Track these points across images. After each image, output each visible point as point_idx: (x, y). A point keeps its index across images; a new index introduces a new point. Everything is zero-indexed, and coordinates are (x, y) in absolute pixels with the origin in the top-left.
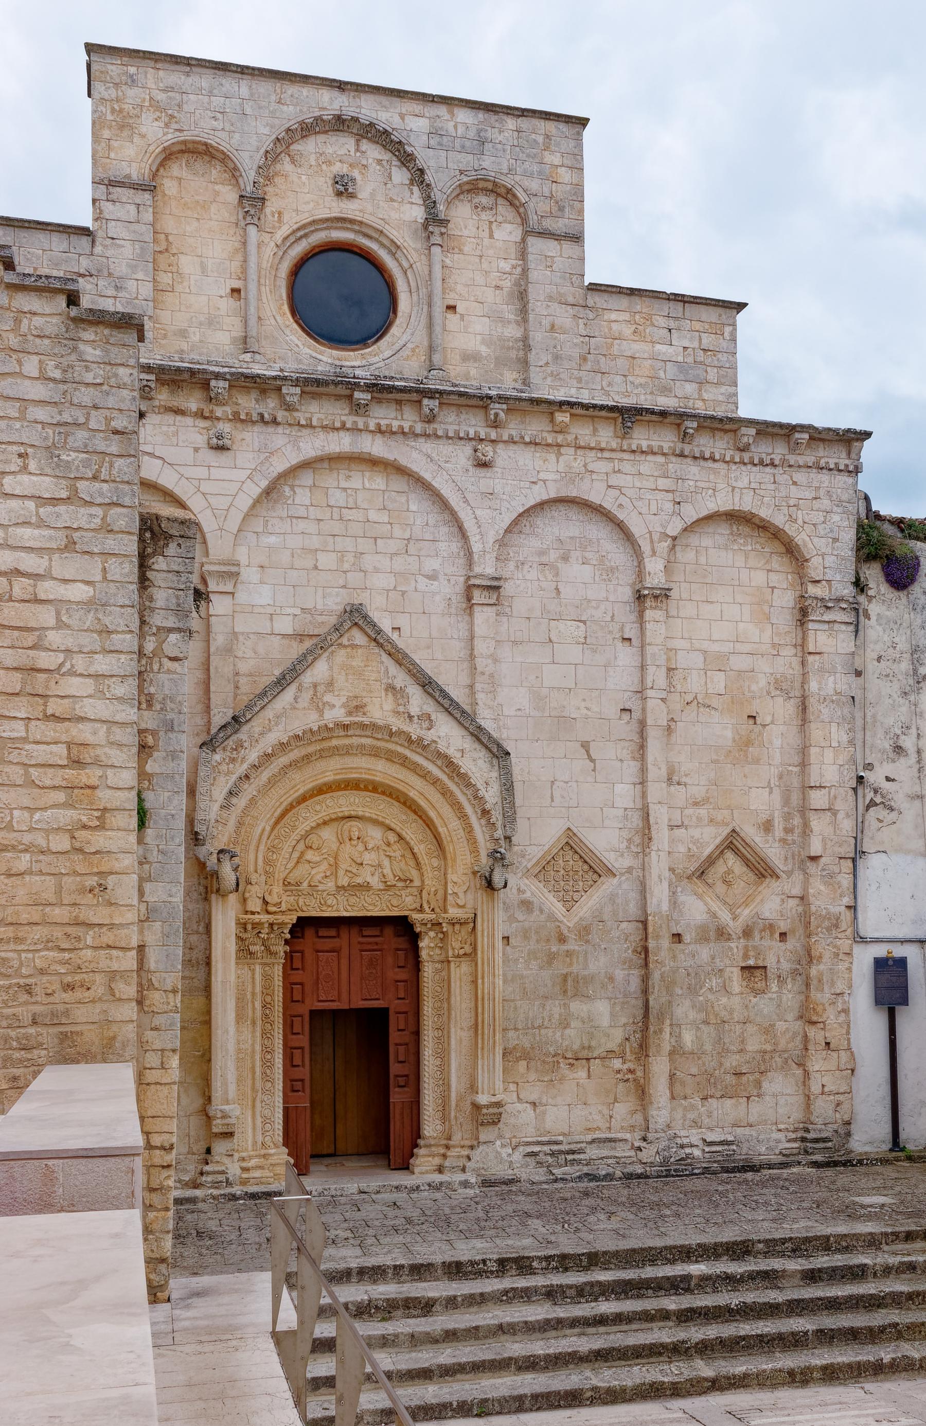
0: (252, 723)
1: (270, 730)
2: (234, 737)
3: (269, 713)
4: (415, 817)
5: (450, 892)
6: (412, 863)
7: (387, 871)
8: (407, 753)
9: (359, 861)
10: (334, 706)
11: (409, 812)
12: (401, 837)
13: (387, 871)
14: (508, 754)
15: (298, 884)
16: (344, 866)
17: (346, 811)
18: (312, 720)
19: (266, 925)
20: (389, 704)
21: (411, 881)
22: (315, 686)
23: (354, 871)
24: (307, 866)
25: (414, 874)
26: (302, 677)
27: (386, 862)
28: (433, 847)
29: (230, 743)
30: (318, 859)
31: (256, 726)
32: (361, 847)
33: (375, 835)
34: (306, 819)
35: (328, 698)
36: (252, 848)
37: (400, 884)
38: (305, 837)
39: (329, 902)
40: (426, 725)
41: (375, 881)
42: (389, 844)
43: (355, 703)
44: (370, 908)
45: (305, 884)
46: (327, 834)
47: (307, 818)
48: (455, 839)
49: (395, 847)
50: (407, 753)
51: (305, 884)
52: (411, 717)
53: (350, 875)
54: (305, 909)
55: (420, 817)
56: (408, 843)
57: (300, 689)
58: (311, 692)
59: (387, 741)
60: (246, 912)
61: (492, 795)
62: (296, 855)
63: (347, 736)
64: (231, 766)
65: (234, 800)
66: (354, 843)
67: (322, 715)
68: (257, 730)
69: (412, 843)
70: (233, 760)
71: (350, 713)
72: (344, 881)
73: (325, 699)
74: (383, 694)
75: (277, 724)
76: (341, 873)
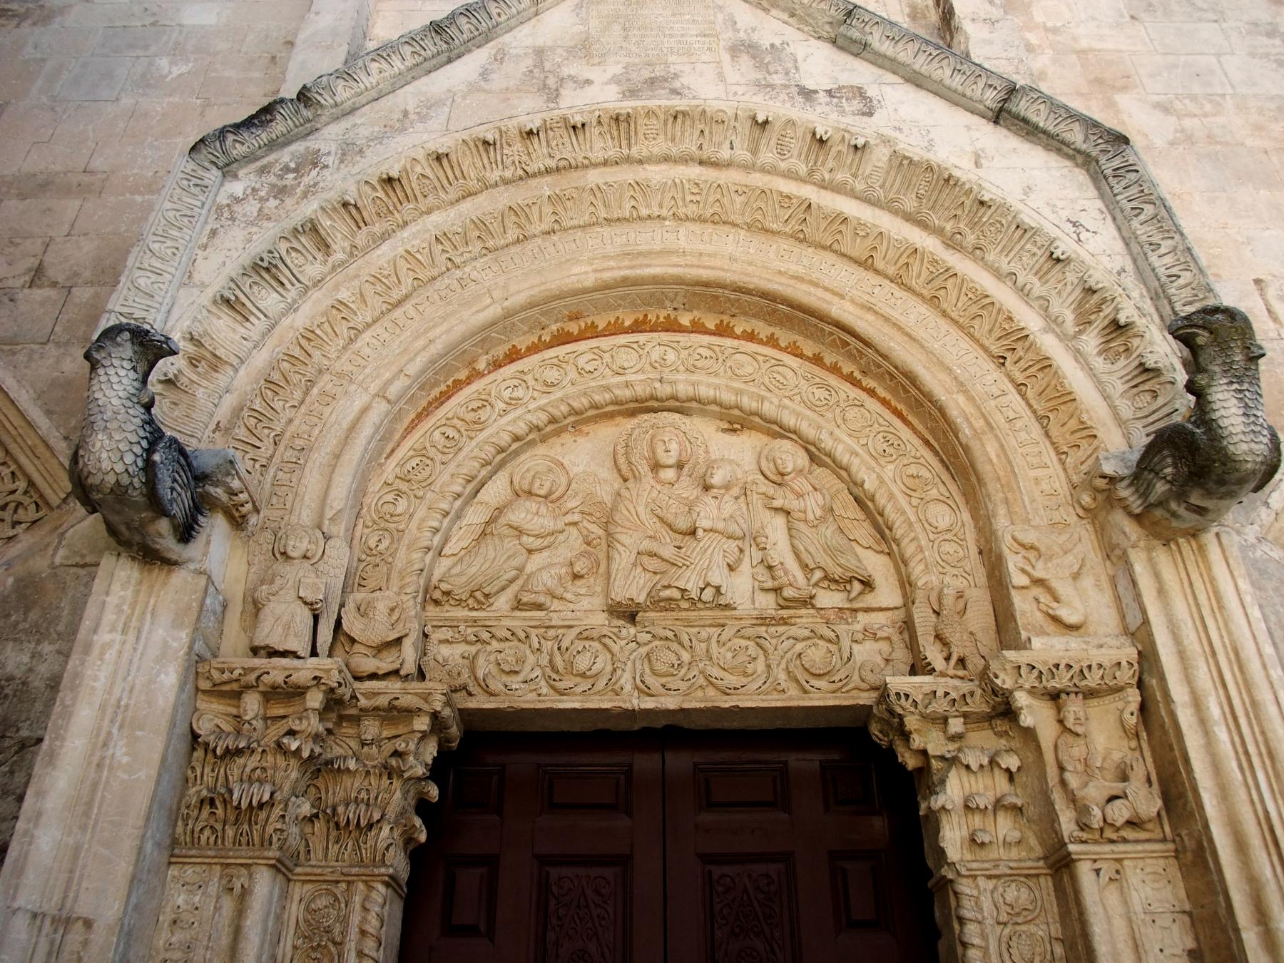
0: (357, 119)
1: (403, 130)
2: (298, 147)
3: (408, 97)
4: (855, 393)
5: (1018, 579)
6: (863, 532)
7: (780, 551)
8: (808, 192)
9: (683, 524)
10: (588, 82)
11: (833, 380)
12: (817, 456)
13: (780, 551)
14: (1121, 140)
15: (480, 597)
16: (630, 542)
17: (640, 383)
18: (529, 111)
19: (315, 699)
20: (741, 72)
21: (868, 584)
22: (540, 52)
23: (668, 552)
24: (511, 544)
25: (876, 565)
26: (507, 38)
27: (776, 529)
28: (927, 465)
29: (285, 156)
30: (549, 524)
31: (363, 125)
32: (687, 489)
33: (737, 454)
34: (513, 403)
35: (571, 69)
36: (319, 458)
37: (829, 599)
38: (504, 456)
39: (583, 663)
40: (856, 104)
41: (742, 589)
42: (780, 479)
43: (646, 74)
44: (732, 680)
45: (502, 602)
46: (585, 457)
47: (515, 396)
48: (999, 419)
49: (800, 484)
50: (808, 192)
51: (502, 602)
52: (807, 94)
53: (653, 564)
54: (495, 685)
55: (871, 392)
56: (839, 469)
57: (500, 57)
58: (529, 62)
59: (748, 168)
60: (255, 651)
61: (1101, 250)
62: (475, 516)
63: (628, 160)
64: (273, 203)
65: (269, 300)
66: (669, 474)
67: (554, 96)
68: (364, 132)
69: (855, 464)
70: (281, 192)
71: (633, 93)
72: (633, 587)
73: (566, 71)
74: (726, 57)
75: (423, 118)
76: (623, 558)
